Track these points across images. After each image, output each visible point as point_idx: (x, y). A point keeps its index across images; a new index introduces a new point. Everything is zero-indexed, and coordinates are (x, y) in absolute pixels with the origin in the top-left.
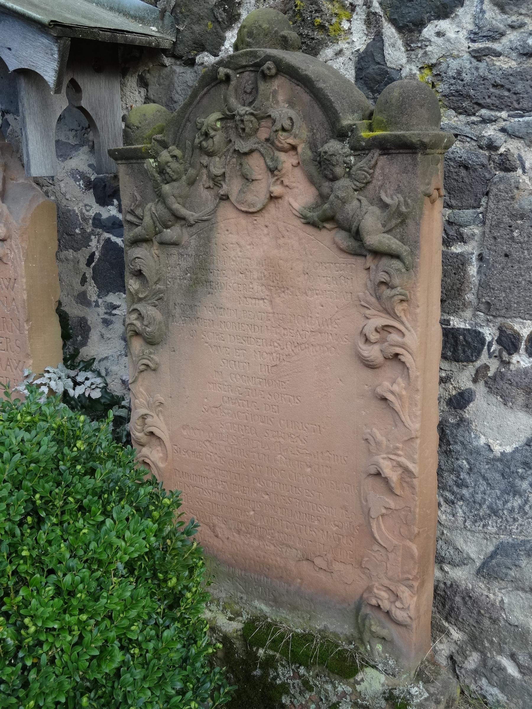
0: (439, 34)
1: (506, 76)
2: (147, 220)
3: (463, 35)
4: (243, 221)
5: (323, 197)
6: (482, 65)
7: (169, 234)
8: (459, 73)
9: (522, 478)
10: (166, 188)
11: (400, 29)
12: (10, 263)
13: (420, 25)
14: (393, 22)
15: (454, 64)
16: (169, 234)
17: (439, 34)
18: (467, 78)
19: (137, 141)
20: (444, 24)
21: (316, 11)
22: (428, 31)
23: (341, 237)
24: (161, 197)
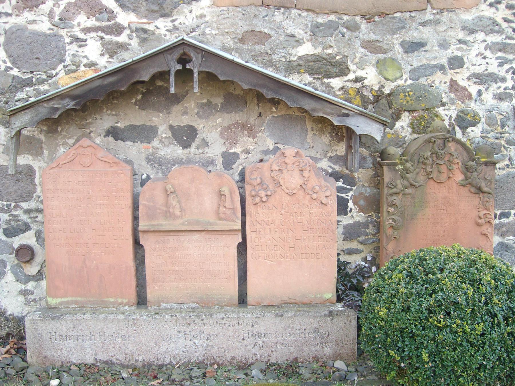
0: (472, 131)
1: (491, 144)
2: (400, 186)
3: (479, 132)
4: (436, 185)
5: (467, 178)
6: (484, 140)
7: (408, 191)
8: (479, 142)
9: (498, 255)
10: (408, 175)
11: (460, 128)
12: (330, 206)
13: (467, 128)
14: (459, 126)
15: (477, 140)
16: (408, 191)
17: (472, 131)
18: (481, 143)
19: (394, 160)
20: (473, 128)
21: (433, 120)
22: (469, 130)
23: (473, 190)
24: (408, 180)
